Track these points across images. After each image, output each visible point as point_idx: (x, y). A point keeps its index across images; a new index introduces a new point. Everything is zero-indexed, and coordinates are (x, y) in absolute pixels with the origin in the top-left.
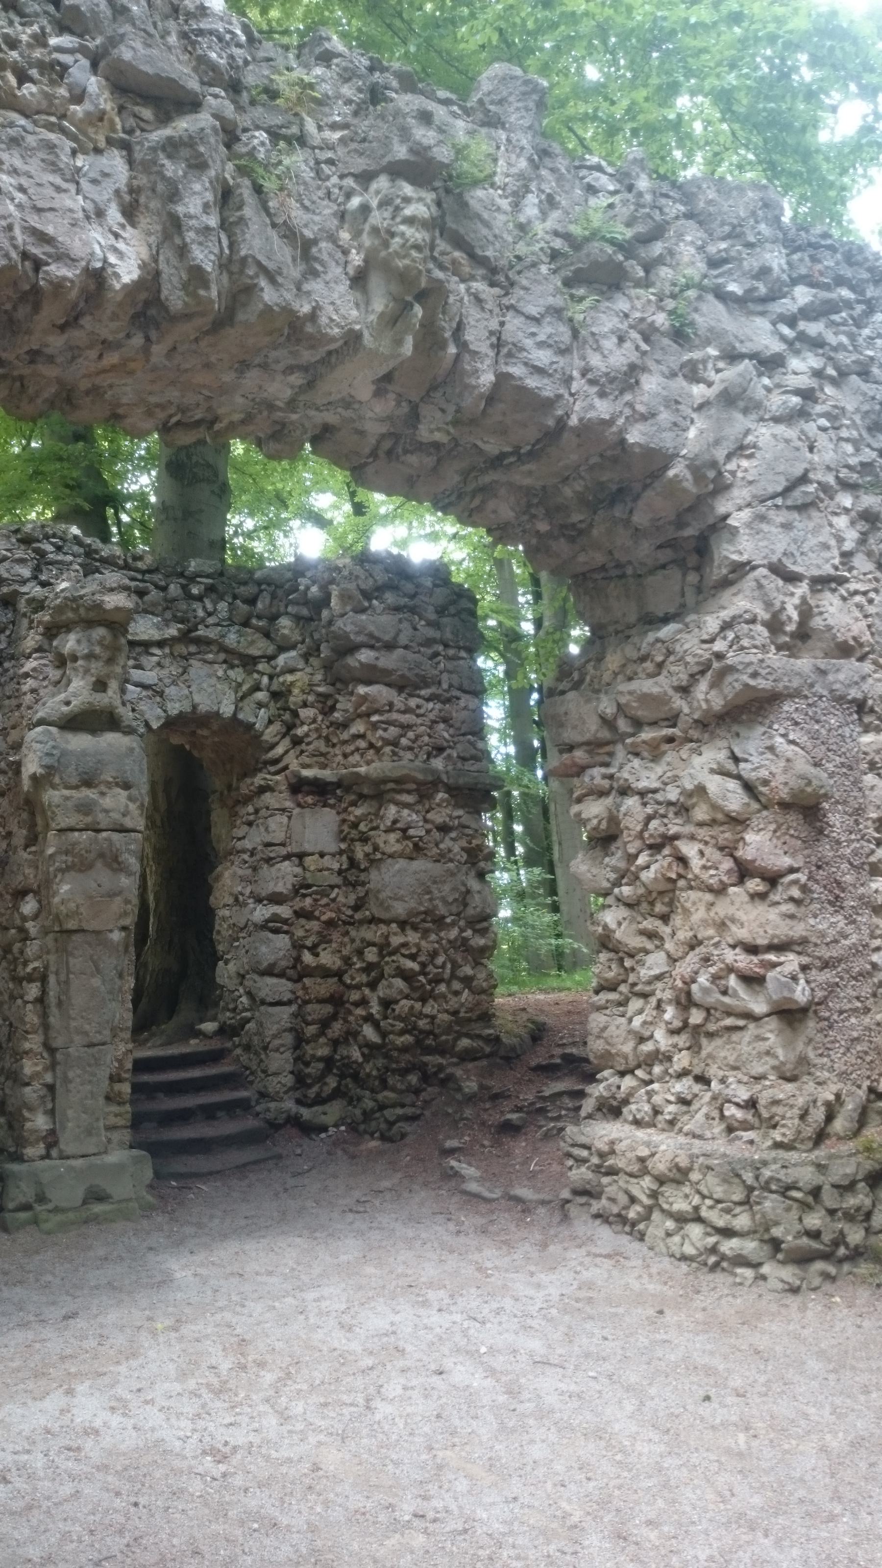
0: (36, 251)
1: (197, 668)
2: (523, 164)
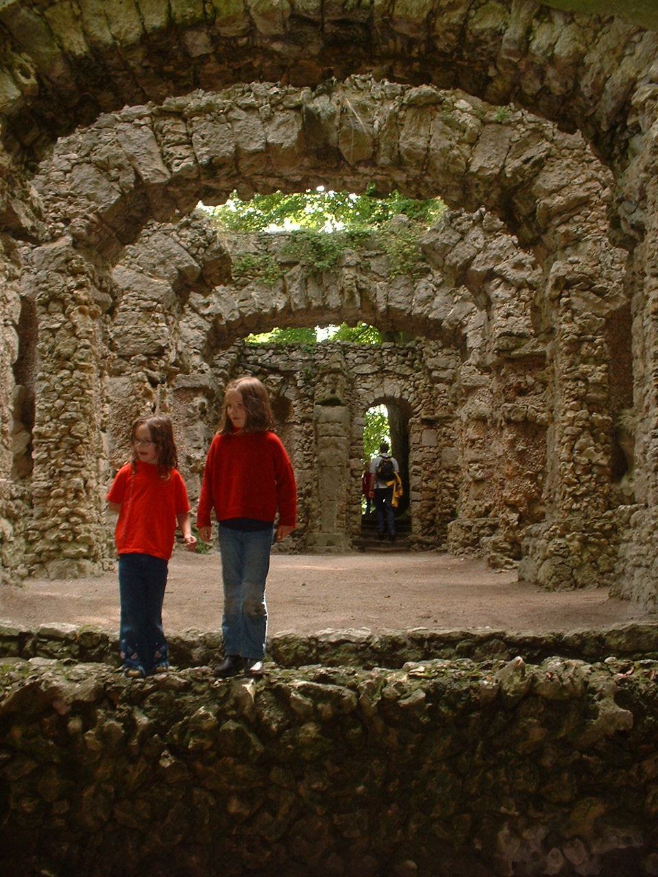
0: (261, 307)
1: (387, 381)
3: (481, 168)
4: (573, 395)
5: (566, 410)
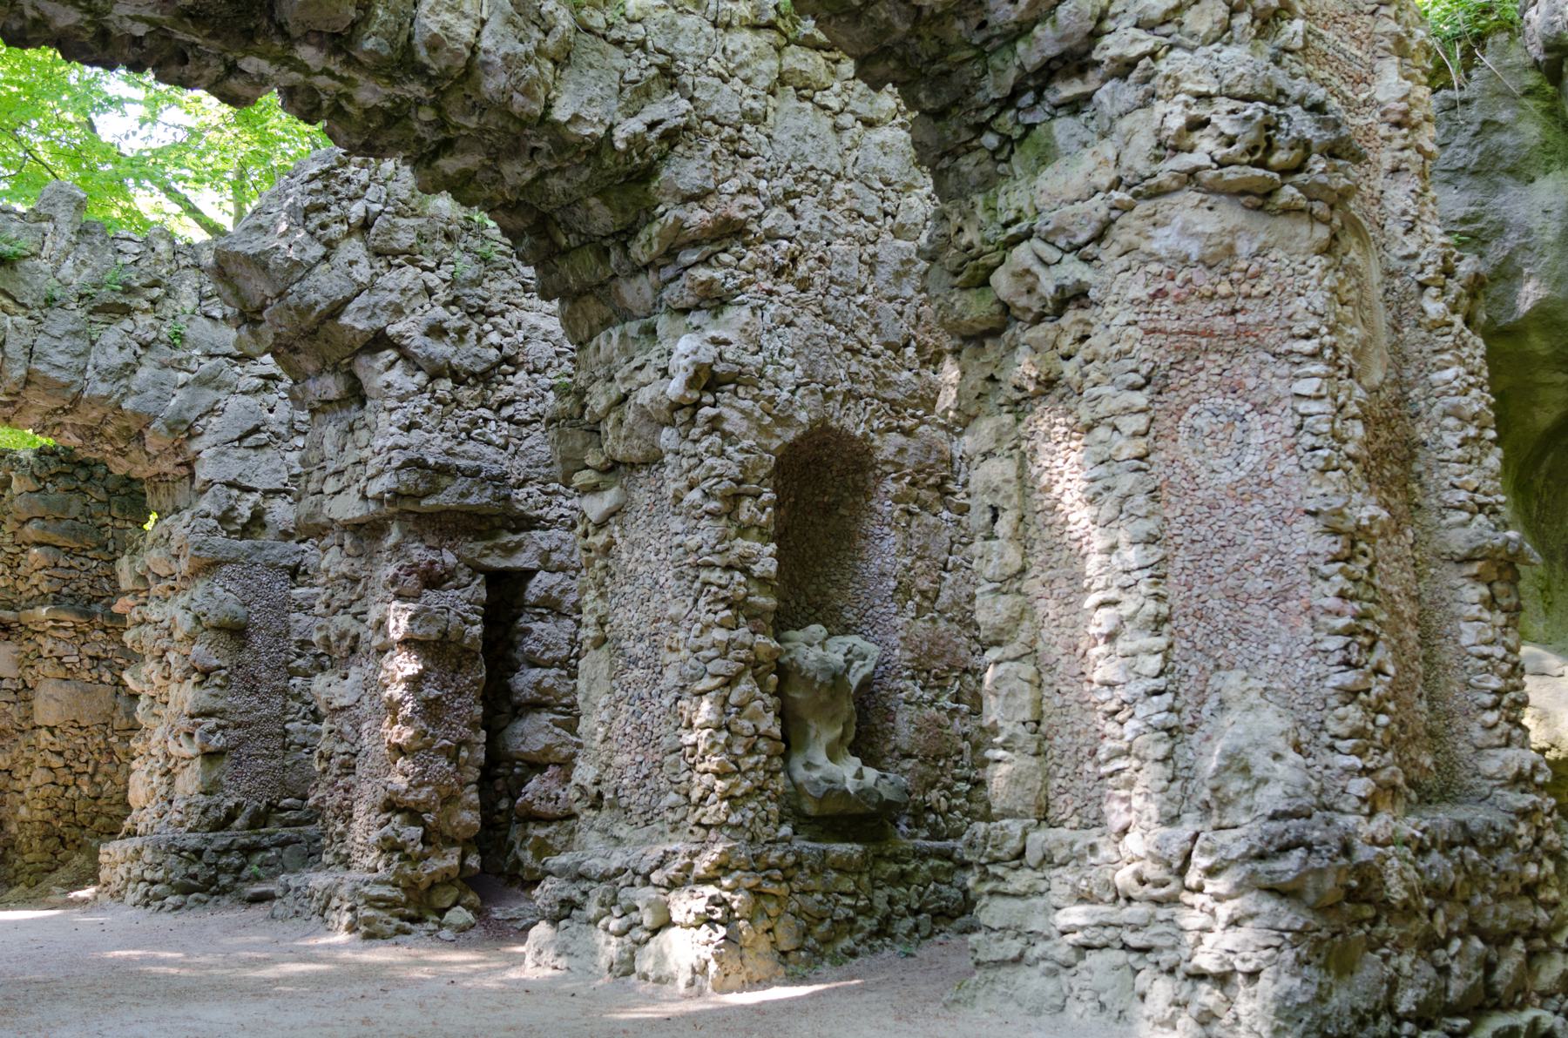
2: (64, 243)
3: (576, 118)
4: (724, 600)
5: (707, 627)
